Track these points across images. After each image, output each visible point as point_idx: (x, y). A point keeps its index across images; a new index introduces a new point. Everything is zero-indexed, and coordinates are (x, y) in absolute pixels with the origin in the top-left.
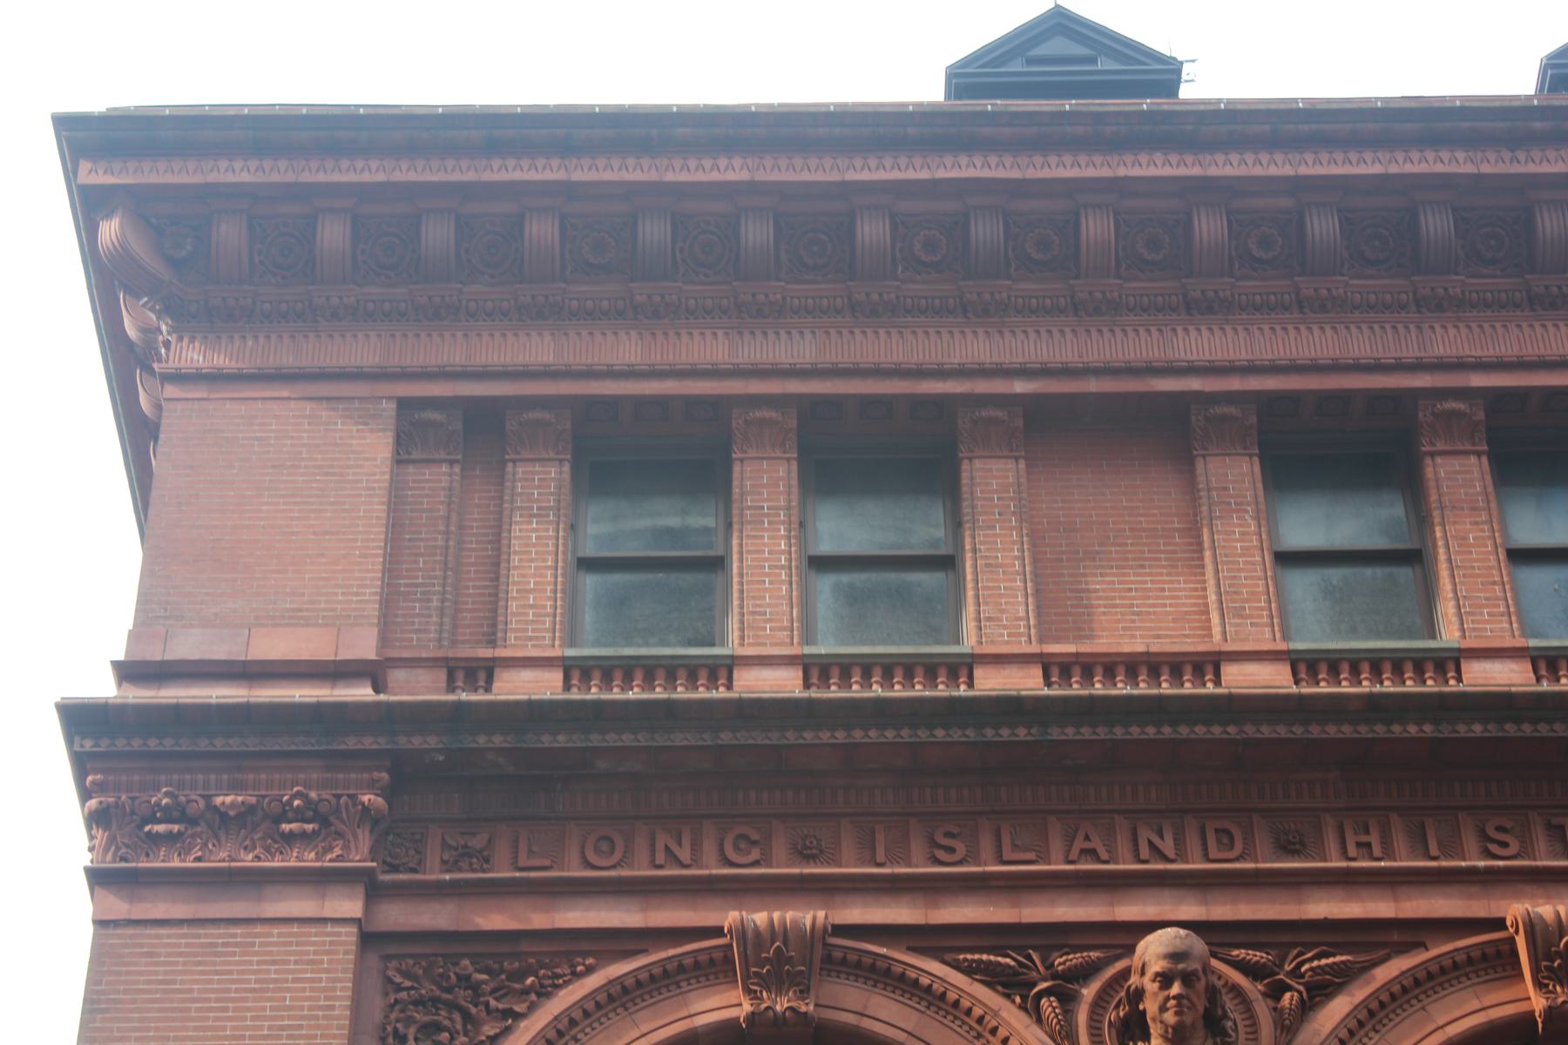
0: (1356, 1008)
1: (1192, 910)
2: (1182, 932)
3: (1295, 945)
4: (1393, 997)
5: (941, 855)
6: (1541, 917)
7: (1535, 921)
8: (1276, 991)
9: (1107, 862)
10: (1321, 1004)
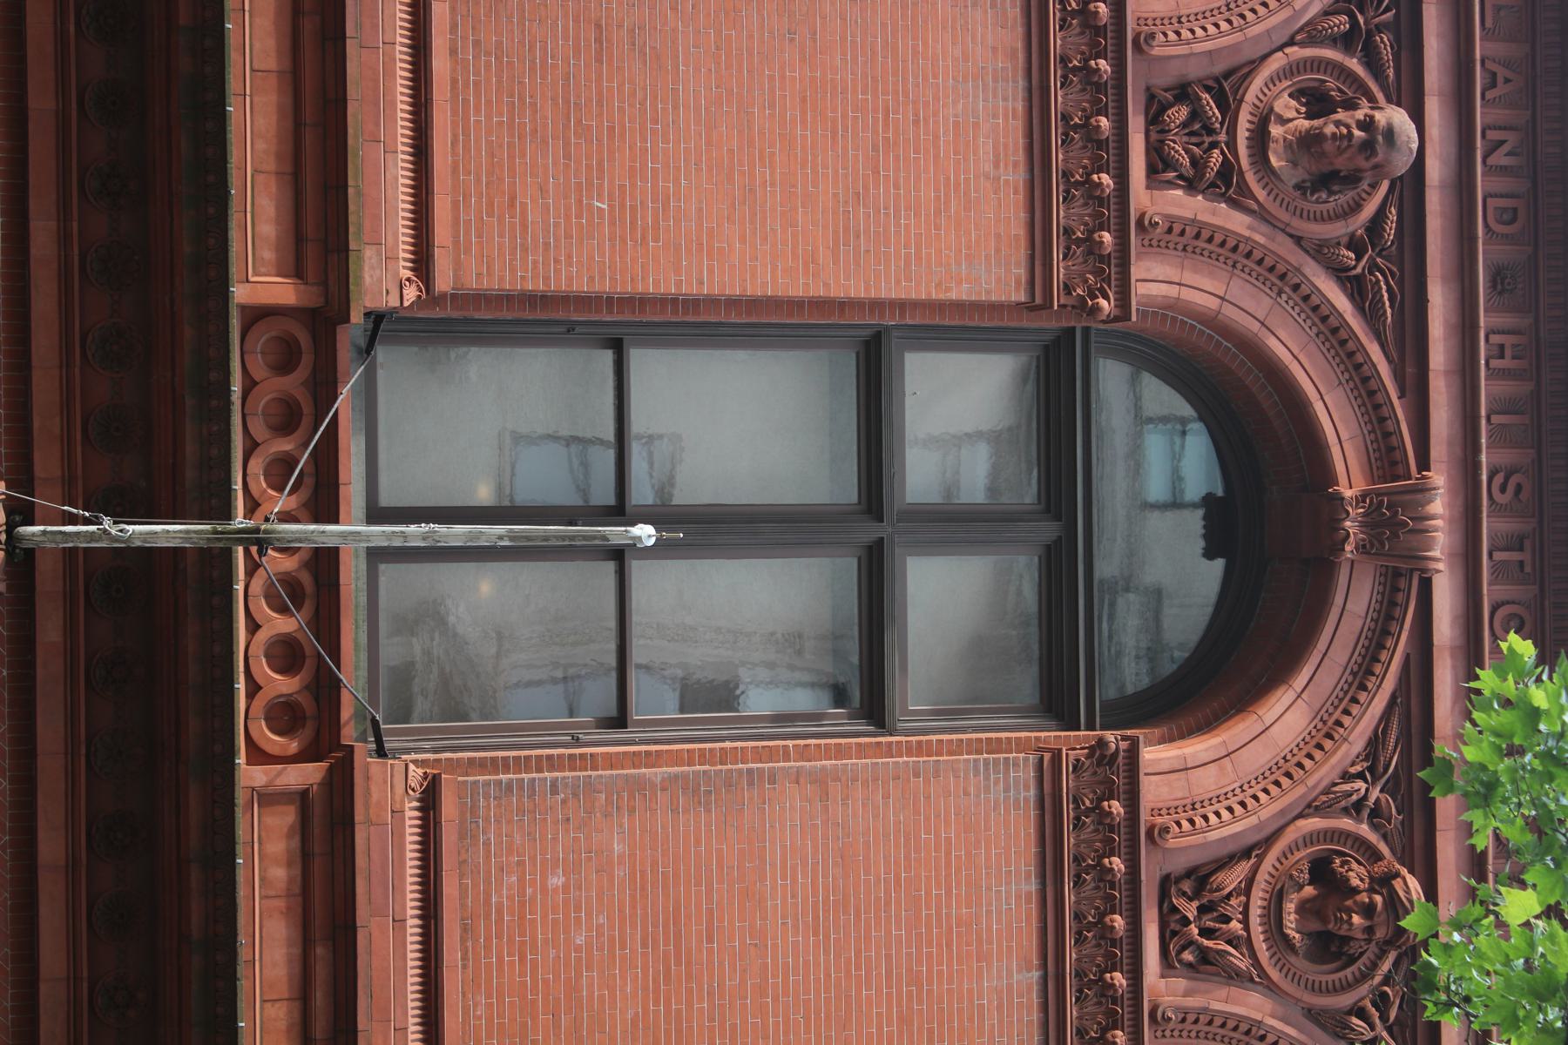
0: (1341, 315)
1: (1436, 171)
2: (1415, 146)
3: (1402, 271)
4: (1351, 355)
5: (1499, 479)
6: (1430, 501)
7: (1427, 495)
8: (1355, 245)
9: (1484, 162)
10: (1344, 290)
